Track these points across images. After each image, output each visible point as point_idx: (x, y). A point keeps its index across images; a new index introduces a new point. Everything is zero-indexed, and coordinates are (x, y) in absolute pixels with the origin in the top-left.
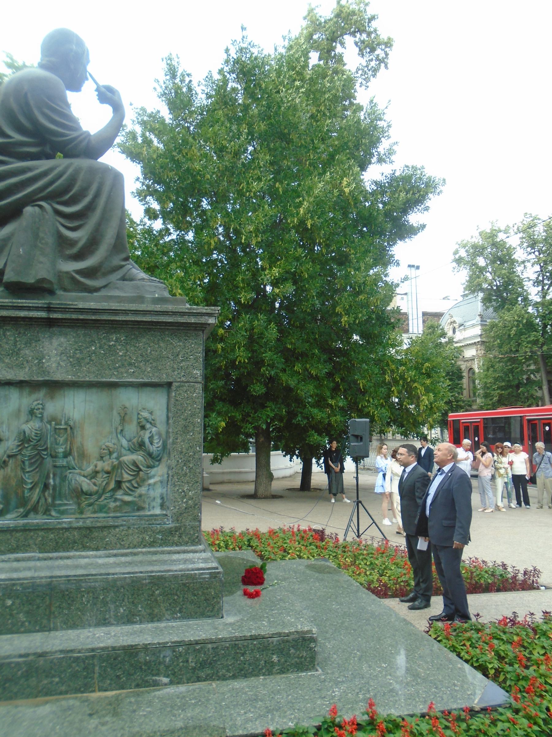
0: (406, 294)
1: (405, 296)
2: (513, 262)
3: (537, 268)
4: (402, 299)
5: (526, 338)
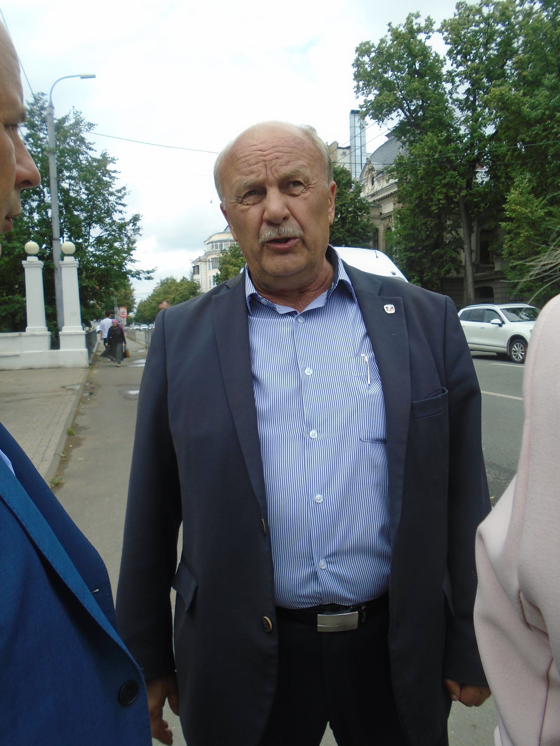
0: (348, 148)
1: (347, 151)
2: (438, 77)
3: (467, 85)
4: (344, 154)
5: (440, 181)
